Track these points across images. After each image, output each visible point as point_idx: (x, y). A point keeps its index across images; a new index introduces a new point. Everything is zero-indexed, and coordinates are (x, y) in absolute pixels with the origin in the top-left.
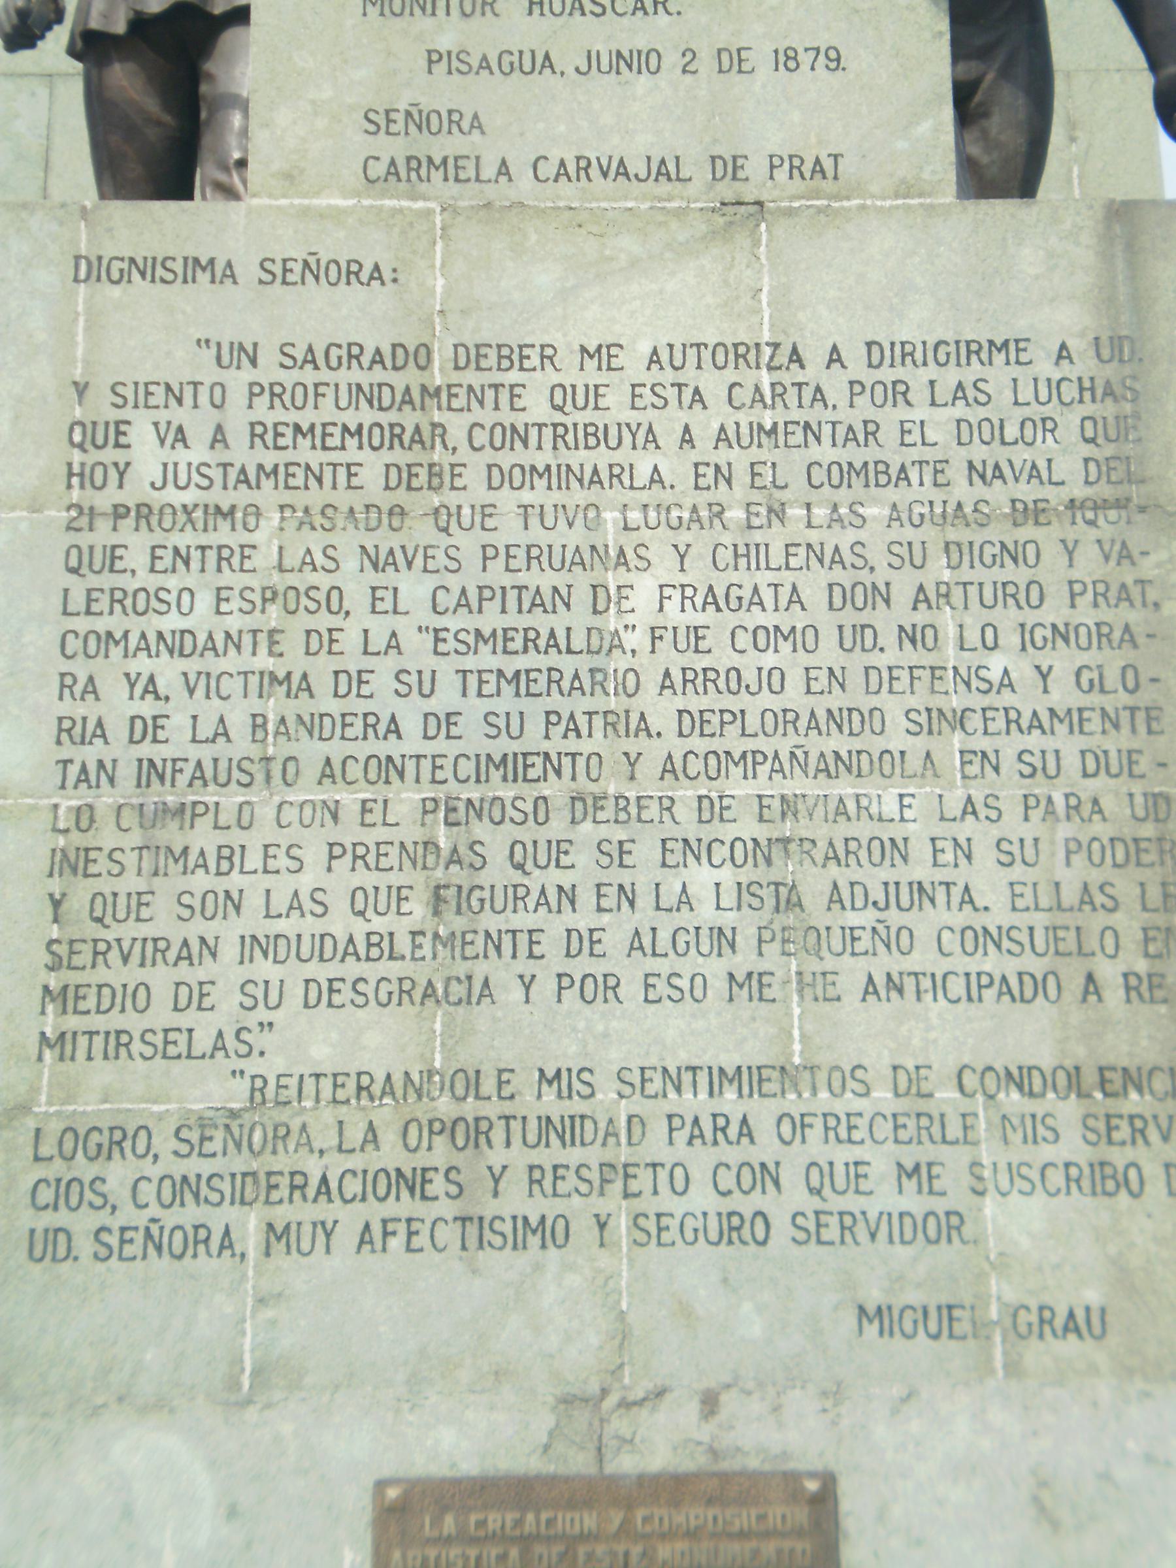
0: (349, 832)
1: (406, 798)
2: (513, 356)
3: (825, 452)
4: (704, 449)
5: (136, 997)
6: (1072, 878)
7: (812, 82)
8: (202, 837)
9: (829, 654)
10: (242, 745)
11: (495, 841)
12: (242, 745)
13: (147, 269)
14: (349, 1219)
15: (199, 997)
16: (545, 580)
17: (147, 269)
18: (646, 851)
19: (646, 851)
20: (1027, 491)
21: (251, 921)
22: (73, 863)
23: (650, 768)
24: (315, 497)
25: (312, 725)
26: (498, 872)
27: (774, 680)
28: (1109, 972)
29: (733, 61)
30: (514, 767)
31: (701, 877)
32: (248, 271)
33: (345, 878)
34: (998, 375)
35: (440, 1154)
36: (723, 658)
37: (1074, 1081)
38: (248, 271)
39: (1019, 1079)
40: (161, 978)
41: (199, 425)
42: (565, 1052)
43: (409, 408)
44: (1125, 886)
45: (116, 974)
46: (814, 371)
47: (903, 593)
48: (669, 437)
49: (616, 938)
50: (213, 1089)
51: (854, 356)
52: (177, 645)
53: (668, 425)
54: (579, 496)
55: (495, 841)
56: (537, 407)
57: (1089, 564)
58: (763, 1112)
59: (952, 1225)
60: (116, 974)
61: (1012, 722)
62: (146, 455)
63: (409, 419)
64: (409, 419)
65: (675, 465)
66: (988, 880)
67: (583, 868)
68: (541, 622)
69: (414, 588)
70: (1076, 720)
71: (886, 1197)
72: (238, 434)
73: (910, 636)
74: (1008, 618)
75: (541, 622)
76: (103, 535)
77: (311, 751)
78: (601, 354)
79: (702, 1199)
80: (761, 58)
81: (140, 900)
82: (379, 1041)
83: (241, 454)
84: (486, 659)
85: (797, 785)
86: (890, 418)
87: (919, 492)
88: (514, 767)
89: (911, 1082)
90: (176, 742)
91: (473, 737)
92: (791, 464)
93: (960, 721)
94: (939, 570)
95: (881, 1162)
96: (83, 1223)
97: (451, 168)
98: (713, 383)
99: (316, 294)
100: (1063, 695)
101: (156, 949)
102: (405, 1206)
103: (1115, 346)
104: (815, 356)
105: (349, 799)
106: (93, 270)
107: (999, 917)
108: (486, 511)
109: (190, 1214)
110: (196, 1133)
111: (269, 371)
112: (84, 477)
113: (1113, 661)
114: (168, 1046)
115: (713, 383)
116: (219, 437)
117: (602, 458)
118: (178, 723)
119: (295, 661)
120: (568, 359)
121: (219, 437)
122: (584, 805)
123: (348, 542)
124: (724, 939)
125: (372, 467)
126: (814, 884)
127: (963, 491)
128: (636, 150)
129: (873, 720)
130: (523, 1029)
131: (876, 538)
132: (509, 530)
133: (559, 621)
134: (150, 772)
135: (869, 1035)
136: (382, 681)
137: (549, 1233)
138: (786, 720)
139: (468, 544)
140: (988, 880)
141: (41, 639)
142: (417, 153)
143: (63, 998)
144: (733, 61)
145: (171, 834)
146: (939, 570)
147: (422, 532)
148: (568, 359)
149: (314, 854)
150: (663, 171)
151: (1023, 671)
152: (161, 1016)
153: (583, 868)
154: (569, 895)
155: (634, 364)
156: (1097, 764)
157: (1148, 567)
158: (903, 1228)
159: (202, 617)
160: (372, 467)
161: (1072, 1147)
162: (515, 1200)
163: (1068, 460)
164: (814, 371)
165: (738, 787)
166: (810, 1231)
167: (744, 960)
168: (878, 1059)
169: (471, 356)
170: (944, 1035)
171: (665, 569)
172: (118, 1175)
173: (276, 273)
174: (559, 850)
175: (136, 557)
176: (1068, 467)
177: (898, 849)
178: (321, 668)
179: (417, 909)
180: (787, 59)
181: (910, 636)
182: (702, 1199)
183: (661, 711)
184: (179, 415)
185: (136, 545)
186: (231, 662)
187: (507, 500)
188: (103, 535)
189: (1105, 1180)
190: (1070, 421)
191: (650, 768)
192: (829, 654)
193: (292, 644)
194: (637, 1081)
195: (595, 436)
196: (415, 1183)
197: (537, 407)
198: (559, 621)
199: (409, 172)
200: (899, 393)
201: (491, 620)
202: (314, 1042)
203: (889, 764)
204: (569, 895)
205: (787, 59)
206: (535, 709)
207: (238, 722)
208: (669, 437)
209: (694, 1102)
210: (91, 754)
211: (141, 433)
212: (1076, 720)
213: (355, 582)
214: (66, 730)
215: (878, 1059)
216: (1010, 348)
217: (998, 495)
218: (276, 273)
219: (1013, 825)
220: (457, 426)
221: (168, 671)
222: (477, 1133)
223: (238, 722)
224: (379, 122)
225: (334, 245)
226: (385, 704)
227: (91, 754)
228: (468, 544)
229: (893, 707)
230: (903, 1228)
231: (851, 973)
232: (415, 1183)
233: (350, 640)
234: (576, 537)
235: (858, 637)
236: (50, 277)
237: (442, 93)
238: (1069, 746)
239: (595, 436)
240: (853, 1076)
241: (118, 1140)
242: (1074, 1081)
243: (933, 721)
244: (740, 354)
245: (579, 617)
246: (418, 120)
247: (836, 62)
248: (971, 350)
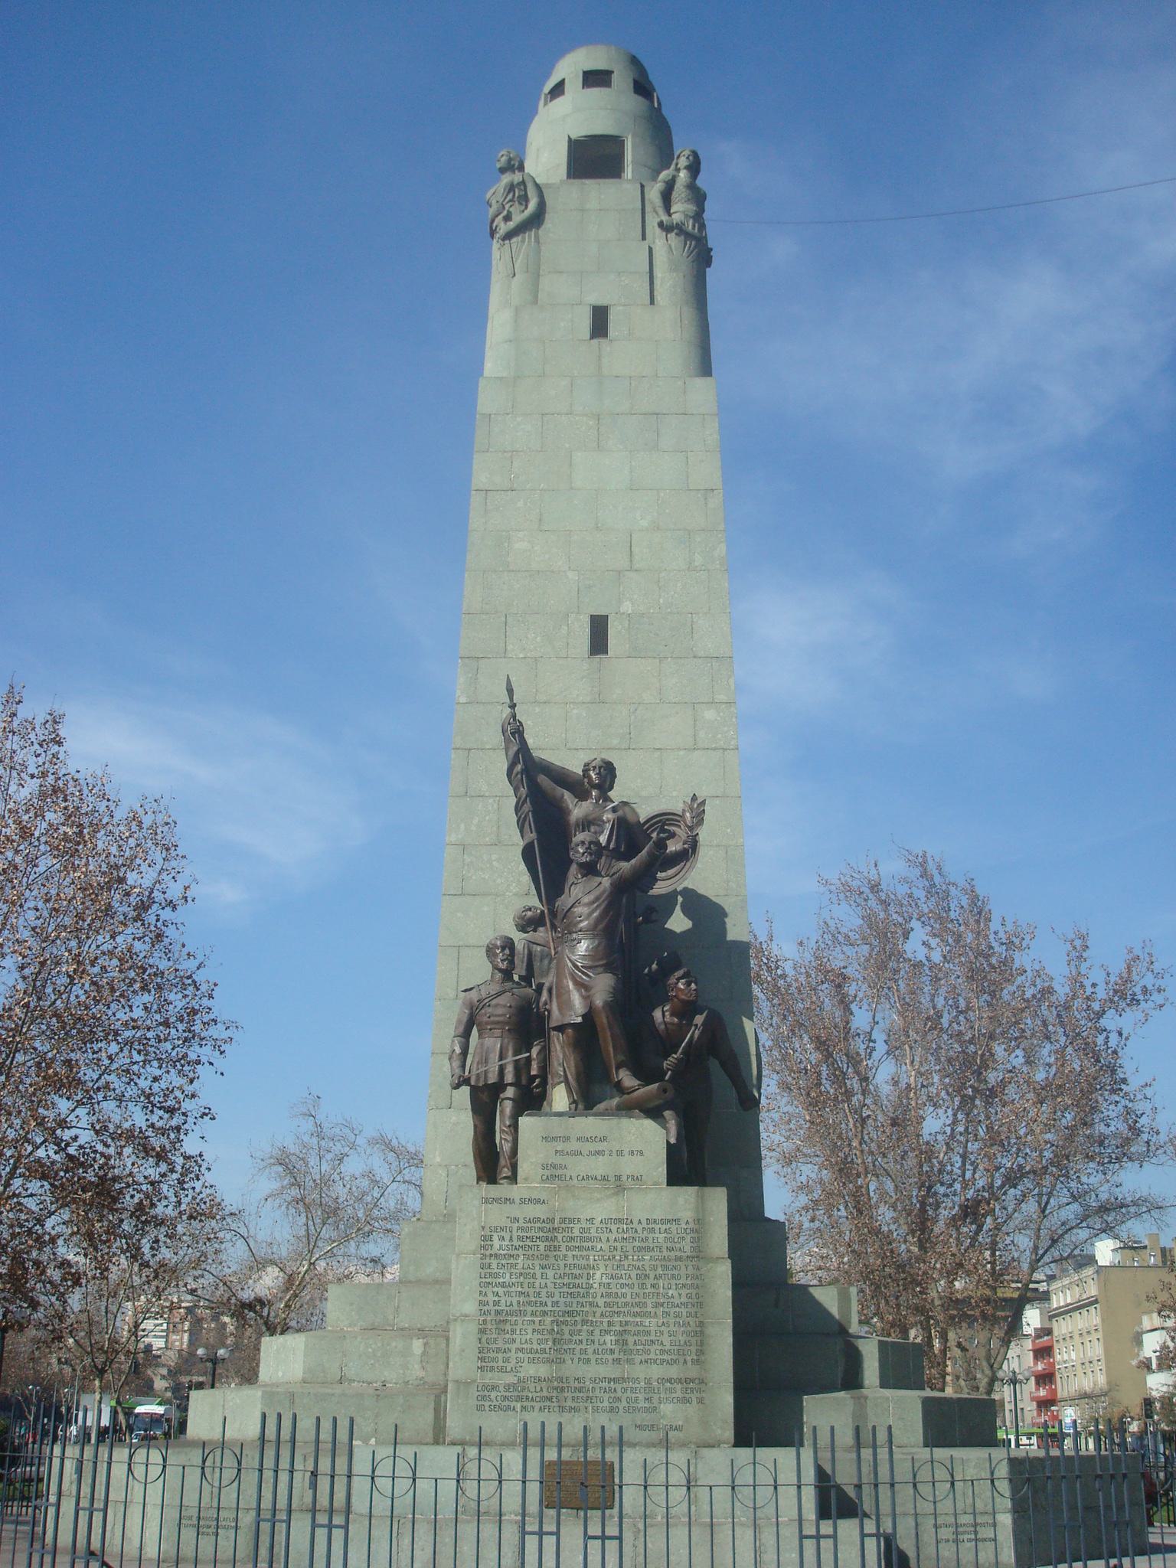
0: (537, 1327)
1: (548, 1320)
2: (572, 1221)
3: (637, 1244)
4: (611, 1243)
5: (496, 1360)
6: (682, 1339)
7: (637, 1159)
8: (508, 1327)
9: (636, 1290)
10: (515, 1307)
11: (566, 1329)
12: (515, 1307)
13: (497, 1200)
14: (537, 1405)
15: (507, 1360)
16: (577, 1272)
17: (497, 1200)
18: (597, 1332)
19: (597, 1332)
20: (678, 1254)
21: (517, 1345)
22: (483, 1331)
23: (598, 1314)
24: (530, 1252)
25: (529, 1303)
26: (567, 1336)
27: (624, 1295)
28: (689, 1359)
29: (620, 1153)
30: (570, 1313)
31: (608, 1338)
32: (517, 1201)
33: (537, 1336)
34: (674, 1227)
35: (555, 1394)
36: (614, 1290)
37: (680, 1381)
38: (517, 1201)
39: (670, 1380)
40: (500, 1356)
41: (507, 1238)
42: (580, 1374)
43: (551, 1234)
44: (693, 1341)
45: (492, 1355)
46: (635, 1225)
47: (652, 1276)
48: (604, 1240)
49: (590, 1351)
50: (511, 1379)
51: (644, 1222)
52: (503, 1284)
53: (604, 1236)
54: (585, 1253)
55: (566, 1329)
56: (576, 1233)
57: (690, 1270)
58: (618, 1387)
59: (655, 1409)
60: (492, 1355)
61: (673, 1306)
62: (496, 1243)
63: (550, 1235)
64: (550, 1235)
65: (605, 1246)
66: (666, 1339)
67: (584, 1336)
68: (577, 1281)
69: (550, 1273)
70: (685, 1305)
71: (642, 1404)
72: (515, 1238)
73: (653, 1286)
74: (673, 1282)
75: (577, 1281)
76: (488, 1261)
77: (529, 1309)
78: (591, 1220)
79: (606, 1404)
80: (626, 1152)
81: (496, 1339)
82: (543, 1370)
83: (516, 1243)
84: (565, 1289)
85: (628, 1319)
86: (651, 1236)
87: (656, 1253)
88: (570, 1313)
89: (648, 1381)
90: (502, 1307)
91: (562, 1308)
92: (629, 1246)
93: (662, 1305)
94: (660, 1271)
95: (641, 1396)
96: (487, 1404)
97: (560, 1177)
98: (614, 1228)
99: (531, 1206)
100: (684, 1300)
101: (499, 1350)
102: (548, 1403)
103: (698, 1221)
104: (635, 1222)
105: (537, 1319)
106: (486, 1201)
107: (668, 1347)
108: (565, 1256)
109: (507, 1403)
110: (507, 1387)
111: (521, 1224)
112: (484, 1247)
113: (694, 1292)
114: (501, 1370)
115: (614, 1228)
116: (511, 1239)
117: (590, 1244)
118: (503, 1302)
119: (526, 1289)
120: (583, 1222)
121: (511, 1239)
122: (585, 1322)
123: (537, 1262)
124: (612, 1351)
125: (542, 1245)
126: (631, 1339)
127: (665, 1253)
128: (600, 1172)
129: (644, 1304)
130: (572, 1369)
131: (647, 1264)
132: (570, 1261)
133: (580, 1281)
134: (497, 1312)
135: (640, 1372)
136: (544, 1294)
137: (576, 1410)
138: (626, 1304)
139: (561, 1263)
140: (666, 1339)
141: (476, 1283)
142: (553, 1174)
143: (482, 1359)
144: (620, 1153)
145: (501, 1326)
146: (660, 1271)
147: (552, 1261)
148: (583, 1222)
149: (530, 1331)
150: (605, 1179)
151: (676, 1294)
152: (500, 1363)
153: (584, 1336)
154: (581, 1341)
155: (597, 1222)
156: (689, 1315)
157: (703, 1271)
158: (646, 1410)
159: (507, 1279)
160: (542, 1245)
161: (679, 1394)
162: (569, 1403)
163: (687, 1246)
164: (635, 1225)
165: (616, 1319)
166: (627, 1410)
167: (616, 1356)
168: (642, 1376)
169: (563, 1220)
170: (656, 1371)
171: (603, 1270)
172: (493, 1395)
173: (523, 1201)
174: (580, 1331)
175: (494, 1266)
176: (687, 1248)
177: (648, 1333)
178: (531, 1291)
179: (550, 1343)
180: (632, 1153)
181: (653, 1286)
182: (606, 1404)
183: (601, 1301)
184: (503, 1234)
185: (494, 1263)
186: (513, 1289)
187: (570, 1253)
188: (488, 1261)
189: (685, 1401)
190: (688, 1239)
191: (598, 1314)
192: (636, 1290)
193: (526, 1286)
194: (593, 1381)
195: (588, 1239)
196: (550, 1399)
197: (576, 1233)
198: (580, 1281)
199: (551, 1178)
200: (653, 1230)
201: (566, 1281)
202: (531, 1370)
203: (647, 1314)
204: (581, 1341)
205: (632, 1153)
206: (575, 1301)
207: (515, 1303)
208: (604, 1240)
209: (604, 1385)
210: (486, 1308)
211: (495, 1238)
212: (685, 1305)
213: (538, 1272)
214: (481, 1303)
215: (642, 1376)
216: (677, 1221)
217: (673, 1254)
218: (523, 1201)
219: (672, 1328)
220: (560, 1236)
221: (501, 1290)
222: (562, 1389)
223: (515, 1303)
224: (545, 1167)
225: (535, 1195)
226: (544, 1299)
227: (486, 1308)
228: (561, 1263)
229: (649, 1302)
230: (646, 1410)
231: (638, 1359)
232: (550, 1399)
233: (537, 1285)
234: (584, 1262)
235: (642, 1286)
236: (477, 1202)
237: (558, 1160)
238: (683, 1310)
239: (588, 1239)
240: (637, 1380)
241: (493, 1388)
242: (680, 1381)
243: (658, 1305)
244: (619, 1221)
245: (584, 1281)
246: (554, 1166)
247: (642, 1154)
248: (668, 1221)
